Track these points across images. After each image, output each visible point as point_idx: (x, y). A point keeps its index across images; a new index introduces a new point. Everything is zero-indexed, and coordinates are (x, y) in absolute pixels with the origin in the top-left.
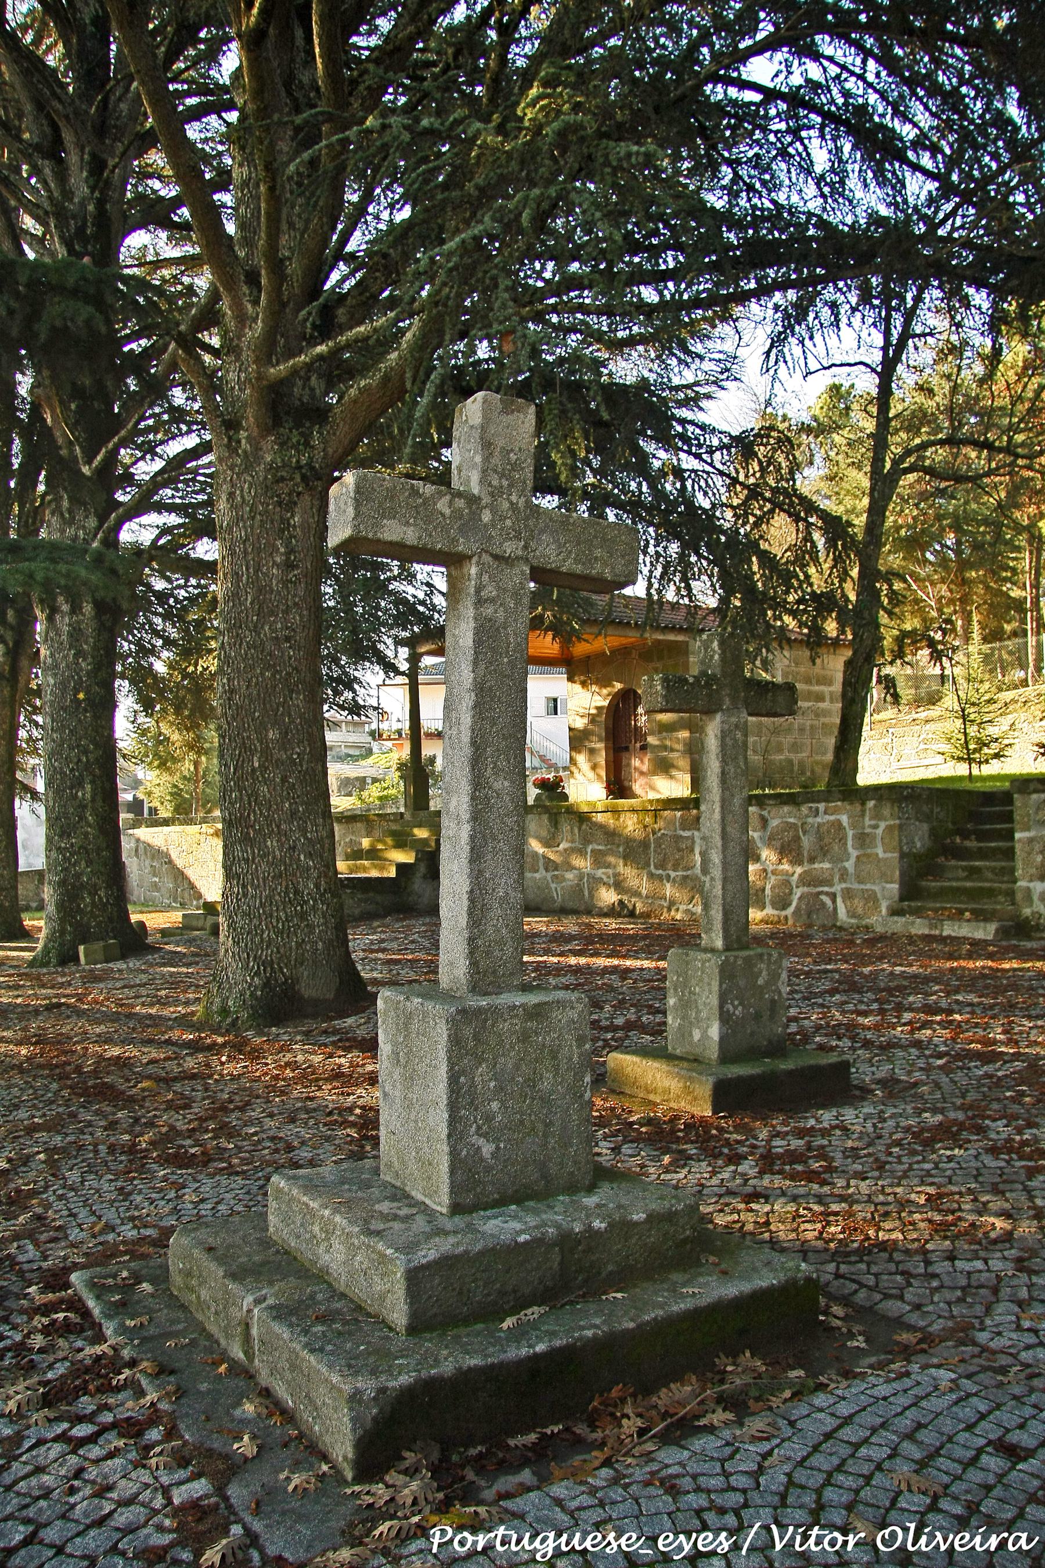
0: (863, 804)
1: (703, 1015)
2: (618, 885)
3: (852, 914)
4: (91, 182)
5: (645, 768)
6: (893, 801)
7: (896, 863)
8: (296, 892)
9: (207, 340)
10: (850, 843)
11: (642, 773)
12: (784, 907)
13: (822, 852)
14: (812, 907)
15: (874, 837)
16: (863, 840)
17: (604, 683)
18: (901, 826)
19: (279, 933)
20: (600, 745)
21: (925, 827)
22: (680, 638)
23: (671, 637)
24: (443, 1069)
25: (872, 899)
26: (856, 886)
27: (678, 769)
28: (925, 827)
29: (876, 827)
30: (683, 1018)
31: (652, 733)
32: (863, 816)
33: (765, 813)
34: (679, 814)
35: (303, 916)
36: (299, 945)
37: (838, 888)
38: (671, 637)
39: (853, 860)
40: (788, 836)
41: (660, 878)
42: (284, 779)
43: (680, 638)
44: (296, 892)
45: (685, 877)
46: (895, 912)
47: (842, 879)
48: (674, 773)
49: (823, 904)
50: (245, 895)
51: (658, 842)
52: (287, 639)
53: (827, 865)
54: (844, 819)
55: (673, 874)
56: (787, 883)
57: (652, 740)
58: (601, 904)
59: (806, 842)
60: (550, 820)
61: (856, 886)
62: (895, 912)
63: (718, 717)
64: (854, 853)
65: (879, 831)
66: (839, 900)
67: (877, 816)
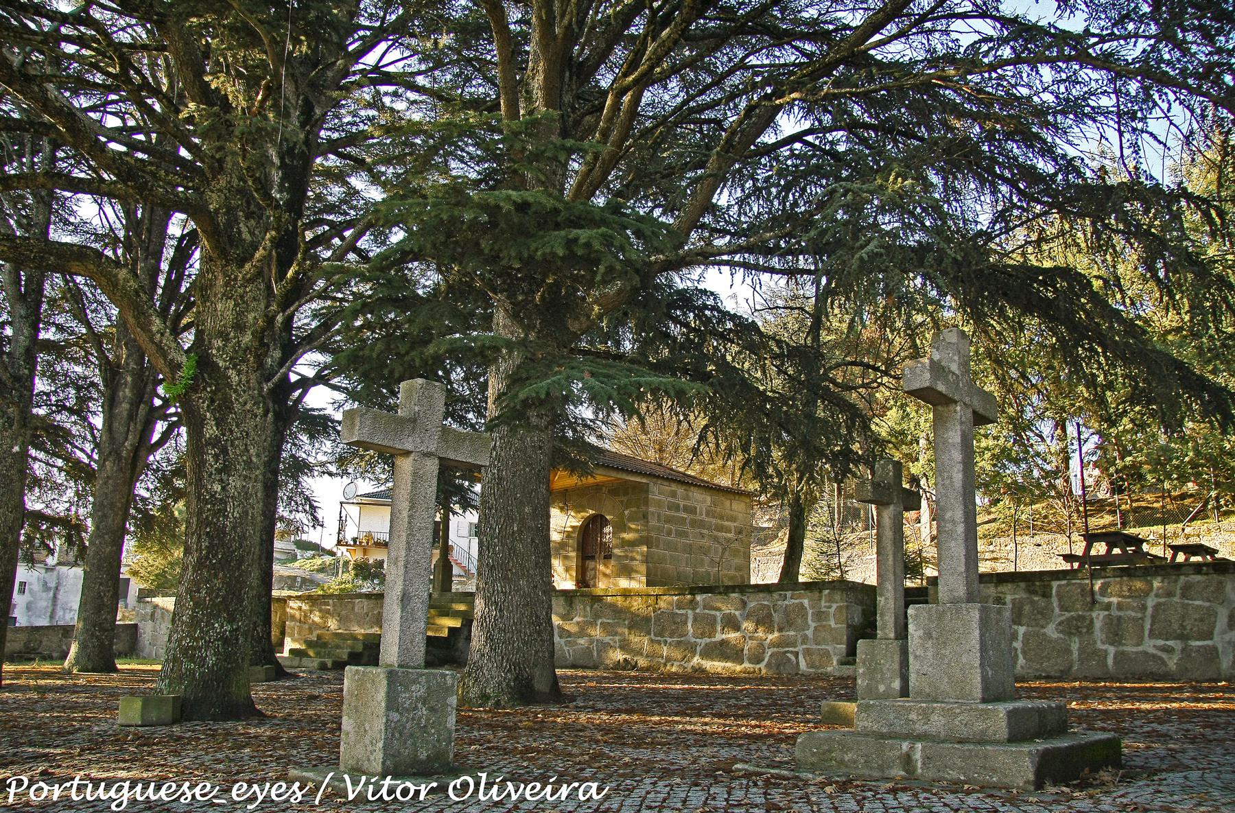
0: (820, 592)
1: (888, 675)
2: (625, 646)
3: (811, 665)
4: (302, 118)
5: (608, 571)
6: (842, 590)
7: (844, 631)
8: (537, 617)
9: (365, 238)
10: (810, 618)
11: (605, 575)
12: (759, 661)
13: (788, 623)
14: (780, 662)
15: (828, 614)
16: (820, 616)
17: (579, 508)
18: (847, 607)
19: (525, 643)
20: (573, 554)
21: (860, 608)
22: (644, 481)
23: (638, 479)
24: (977, 633)
25: (826, 654)
26: (814, 647)
27: (637, 572)
28: (860, 608)
29: (830, 607)
30: (870, 680)
31: (617, 547)
32: (820, 600)
33: (745, 598)
34: (675, 598)
35: (539, 633)
36: (536, 652)
37: (800, 648)
38: (638, 479)
39: (812, 629)
40: (762, 613)
41: (659, 642)
42: (533, 540)
43: (644, 481)
44: (537, 617)
45: (679, 643)
46: (842, 663)
47: (803, 642)
48: (634, 575)
49: (789, 660)
50: (502, 617)
51: (658, 619)
52: (540, 448)
53: (792, 633)
54: (806, 602)
55: (669, 640)
56: (761, 645)
57: (617, 551)
58: (608, 662)
59: (776, 617)
60: (566, 601)
61: (814, 647)
62: (842, 663)
63: (892, 507)
64: (813, 625)
65: (832, 610)
66: (801, 657)
67: (831, 600)
